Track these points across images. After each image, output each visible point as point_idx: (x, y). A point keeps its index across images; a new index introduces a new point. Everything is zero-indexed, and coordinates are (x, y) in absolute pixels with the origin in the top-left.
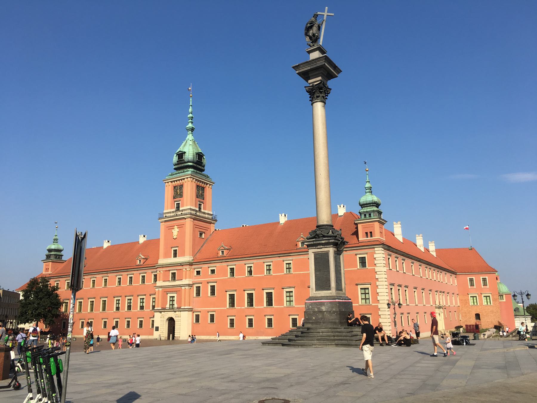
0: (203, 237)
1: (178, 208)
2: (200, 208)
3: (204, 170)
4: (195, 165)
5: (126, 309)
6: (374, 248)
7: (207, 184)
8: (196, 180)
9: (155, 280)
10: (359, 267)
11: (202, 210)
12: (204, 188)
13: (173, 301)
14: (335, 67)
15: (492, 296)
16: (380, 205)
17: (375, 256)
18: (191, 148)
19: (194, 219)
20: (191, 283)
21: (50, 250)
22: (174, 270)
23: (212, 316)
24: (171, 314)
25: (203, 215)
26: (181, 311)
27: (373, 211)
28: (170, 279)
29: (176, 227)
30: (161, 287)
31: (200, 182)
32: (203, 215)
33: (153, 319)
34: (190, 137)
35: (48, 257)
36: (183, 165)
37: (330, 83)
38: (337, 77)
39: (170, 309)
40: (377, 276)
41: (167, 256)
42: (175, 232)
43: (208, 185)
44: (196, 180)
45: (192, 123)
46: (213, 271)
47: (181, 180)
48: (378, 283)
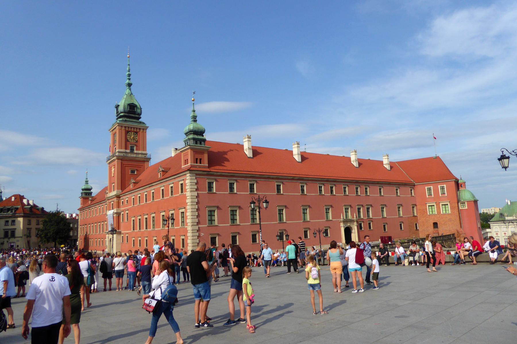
2: (132, 150)
4: (127, 114)
6: (186, 174)
7: (140, 129)
8: (125, 127)
11: (135, 152)
12: (137, 133)
15: (450, 204)
18: (123, 101)
19: (122, 160)
20: (119, 211)
21: (83, 190)
25: (135, 155)
27: (189, 139)
32: (135, 155)
34: (127, 91)
41: (110, 191)
43: (142, 131)
44: (125, 127)
45: (129, 79)
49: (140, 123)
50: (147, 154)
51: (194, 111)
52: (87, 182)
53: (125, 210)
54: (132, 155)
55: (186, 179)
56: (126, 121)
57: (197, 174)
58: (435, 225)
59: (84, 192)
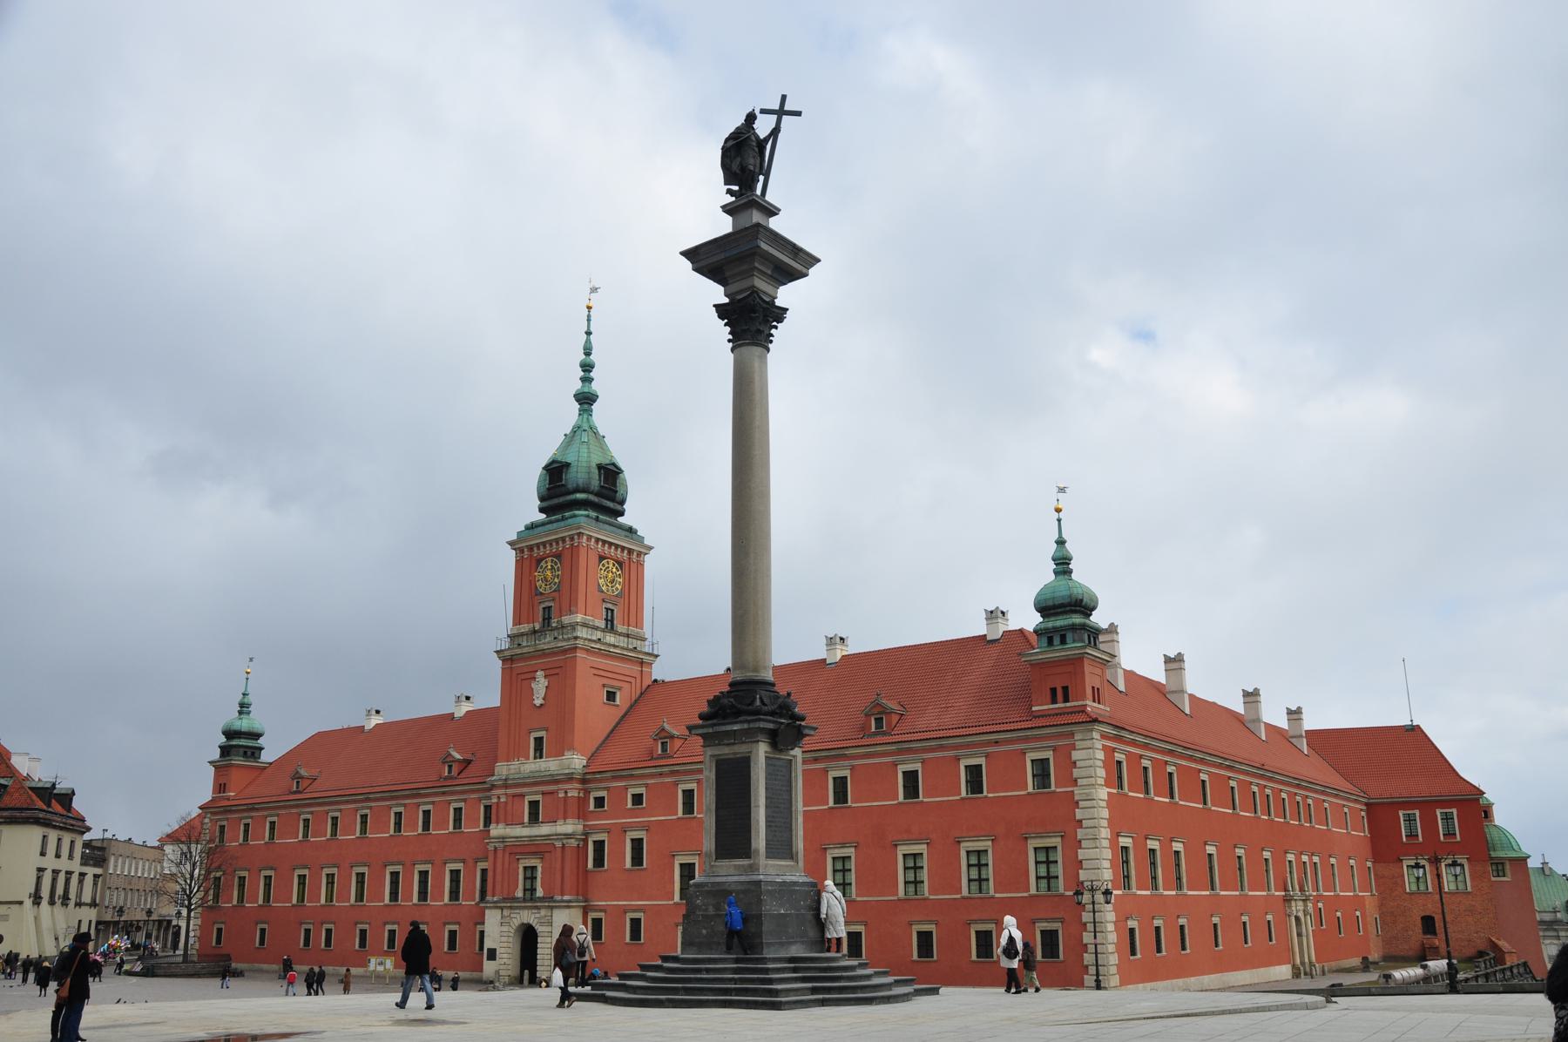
0: (618, 702)
1: (547, 620)
2: (610, 621)
3: (622, 514)
5: (415, 900)
6: (1072, 734)
7: (630, 551)
8: (598, 540)
9: (488, 821)
10: (1030, 789)
13: (533, 878)
14: (795, 251)
16: (1094, 609)
17: (1076, 755)
21: (230, 734)
22: (536, 793)
23: (636, 923)
24: (528, 917)
26: (552, 908)
28: (526, 819)
29: (540, 674)
30: (503, 839)
31: (611, 544)
33: (479, 928)
35: (225, 751)
36: (561, 500)
37: (785, 295)
38: (806, 275)
39: (524, 900)
40: (1079, 814)
42: (540, 686)
46: (637, 799)
47: (557, 541)
48: (1080, 833)
49: (631, 530)
50: (644, 640)
51: (1061, 542)
52: (244, 708)
53: (633, 827)
54: (610, 639)
55: (1074, 747)
56: (597, 519)
57: (1104, 737)
58: (1428, 924)
59: (234, 742)
